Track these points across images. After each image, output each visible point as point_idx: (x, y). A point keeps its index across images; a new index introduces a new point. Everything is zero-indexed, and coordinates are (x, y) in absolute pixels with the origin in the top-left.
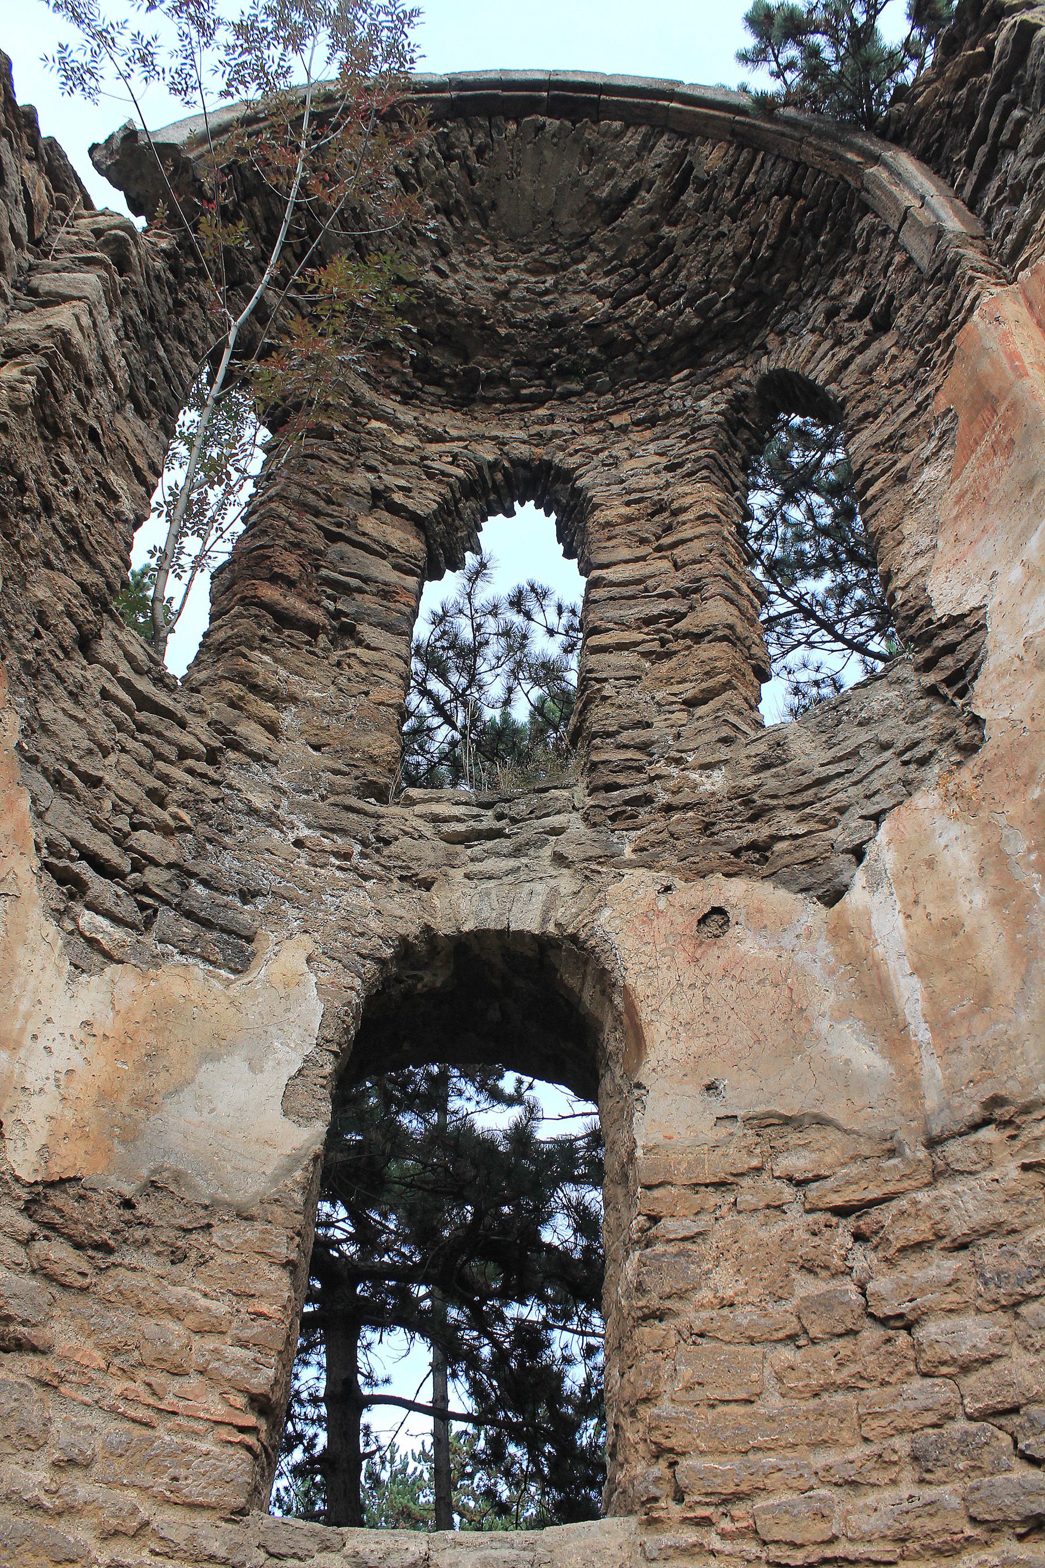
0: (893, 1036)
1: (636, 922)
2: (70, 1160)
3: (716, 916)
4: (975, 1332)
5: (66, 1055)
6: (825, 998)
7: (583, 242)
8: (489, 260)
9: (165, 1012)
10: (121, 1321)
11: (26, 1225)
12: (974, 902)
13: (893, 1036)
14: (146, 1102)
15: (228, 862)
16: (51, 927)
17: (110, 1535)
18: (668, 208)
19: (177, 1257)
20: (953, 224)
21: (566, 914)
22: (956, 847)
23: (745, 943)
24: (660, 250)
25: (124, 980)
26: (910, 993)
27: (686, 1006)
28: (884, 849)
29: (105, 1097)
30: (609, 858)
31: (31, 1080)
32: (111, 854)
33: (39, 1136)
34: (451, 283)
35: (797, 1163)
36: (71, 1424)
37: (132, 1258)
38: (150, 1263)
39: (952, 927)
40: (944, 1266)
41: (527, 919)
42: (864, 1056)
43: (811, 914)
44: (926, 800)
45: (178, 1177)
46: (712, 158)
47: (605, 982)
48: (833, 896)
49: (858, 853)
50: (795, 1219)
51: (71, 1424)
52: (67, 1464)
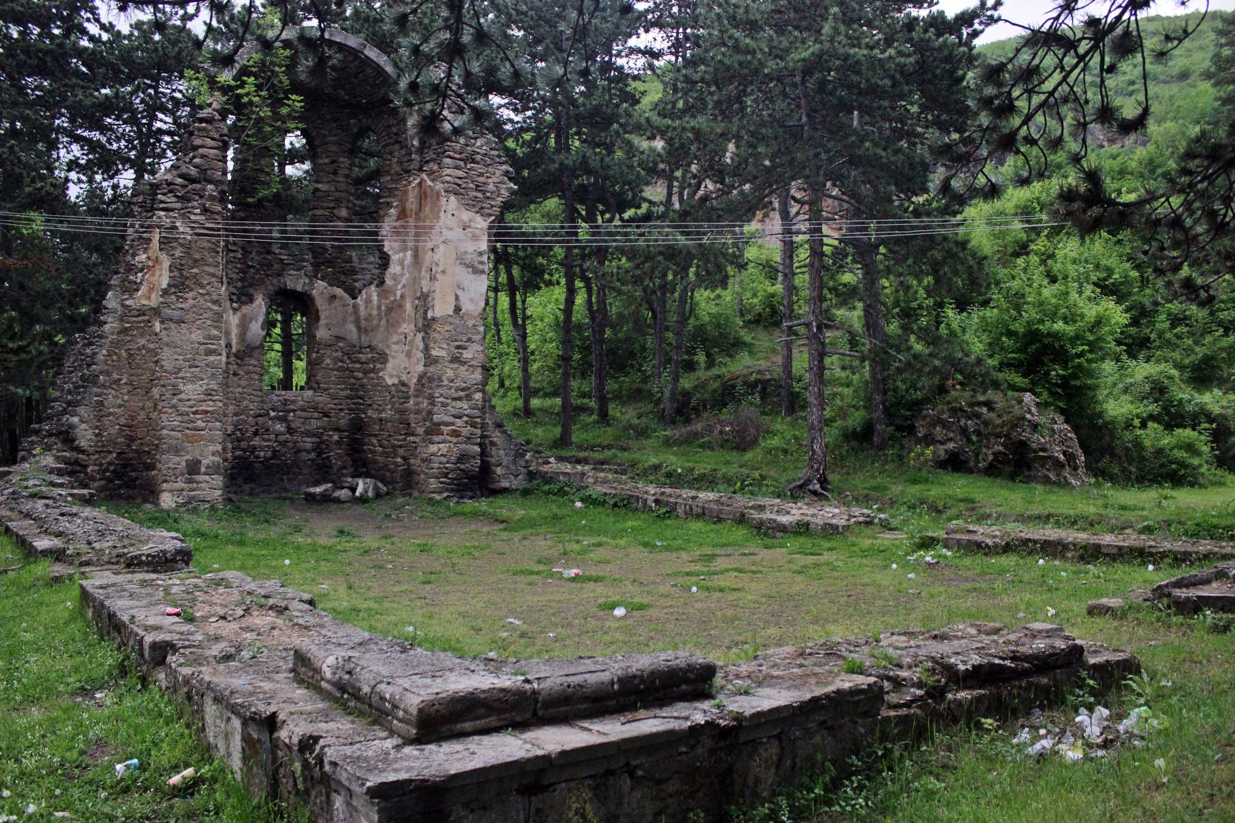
3: (334, 297)
4: (360, 375)
10: (246, 368)
12: (375, 312)
27: (327, 313)
35: (341, 344)
36: (243, 383)
39: (370, 315)
40: (358, 366)
41: (299, 288)
44: (373, 288)
48: (355, 298)
49: (360, 292)
50: (339, 354)
51: (243, 383)
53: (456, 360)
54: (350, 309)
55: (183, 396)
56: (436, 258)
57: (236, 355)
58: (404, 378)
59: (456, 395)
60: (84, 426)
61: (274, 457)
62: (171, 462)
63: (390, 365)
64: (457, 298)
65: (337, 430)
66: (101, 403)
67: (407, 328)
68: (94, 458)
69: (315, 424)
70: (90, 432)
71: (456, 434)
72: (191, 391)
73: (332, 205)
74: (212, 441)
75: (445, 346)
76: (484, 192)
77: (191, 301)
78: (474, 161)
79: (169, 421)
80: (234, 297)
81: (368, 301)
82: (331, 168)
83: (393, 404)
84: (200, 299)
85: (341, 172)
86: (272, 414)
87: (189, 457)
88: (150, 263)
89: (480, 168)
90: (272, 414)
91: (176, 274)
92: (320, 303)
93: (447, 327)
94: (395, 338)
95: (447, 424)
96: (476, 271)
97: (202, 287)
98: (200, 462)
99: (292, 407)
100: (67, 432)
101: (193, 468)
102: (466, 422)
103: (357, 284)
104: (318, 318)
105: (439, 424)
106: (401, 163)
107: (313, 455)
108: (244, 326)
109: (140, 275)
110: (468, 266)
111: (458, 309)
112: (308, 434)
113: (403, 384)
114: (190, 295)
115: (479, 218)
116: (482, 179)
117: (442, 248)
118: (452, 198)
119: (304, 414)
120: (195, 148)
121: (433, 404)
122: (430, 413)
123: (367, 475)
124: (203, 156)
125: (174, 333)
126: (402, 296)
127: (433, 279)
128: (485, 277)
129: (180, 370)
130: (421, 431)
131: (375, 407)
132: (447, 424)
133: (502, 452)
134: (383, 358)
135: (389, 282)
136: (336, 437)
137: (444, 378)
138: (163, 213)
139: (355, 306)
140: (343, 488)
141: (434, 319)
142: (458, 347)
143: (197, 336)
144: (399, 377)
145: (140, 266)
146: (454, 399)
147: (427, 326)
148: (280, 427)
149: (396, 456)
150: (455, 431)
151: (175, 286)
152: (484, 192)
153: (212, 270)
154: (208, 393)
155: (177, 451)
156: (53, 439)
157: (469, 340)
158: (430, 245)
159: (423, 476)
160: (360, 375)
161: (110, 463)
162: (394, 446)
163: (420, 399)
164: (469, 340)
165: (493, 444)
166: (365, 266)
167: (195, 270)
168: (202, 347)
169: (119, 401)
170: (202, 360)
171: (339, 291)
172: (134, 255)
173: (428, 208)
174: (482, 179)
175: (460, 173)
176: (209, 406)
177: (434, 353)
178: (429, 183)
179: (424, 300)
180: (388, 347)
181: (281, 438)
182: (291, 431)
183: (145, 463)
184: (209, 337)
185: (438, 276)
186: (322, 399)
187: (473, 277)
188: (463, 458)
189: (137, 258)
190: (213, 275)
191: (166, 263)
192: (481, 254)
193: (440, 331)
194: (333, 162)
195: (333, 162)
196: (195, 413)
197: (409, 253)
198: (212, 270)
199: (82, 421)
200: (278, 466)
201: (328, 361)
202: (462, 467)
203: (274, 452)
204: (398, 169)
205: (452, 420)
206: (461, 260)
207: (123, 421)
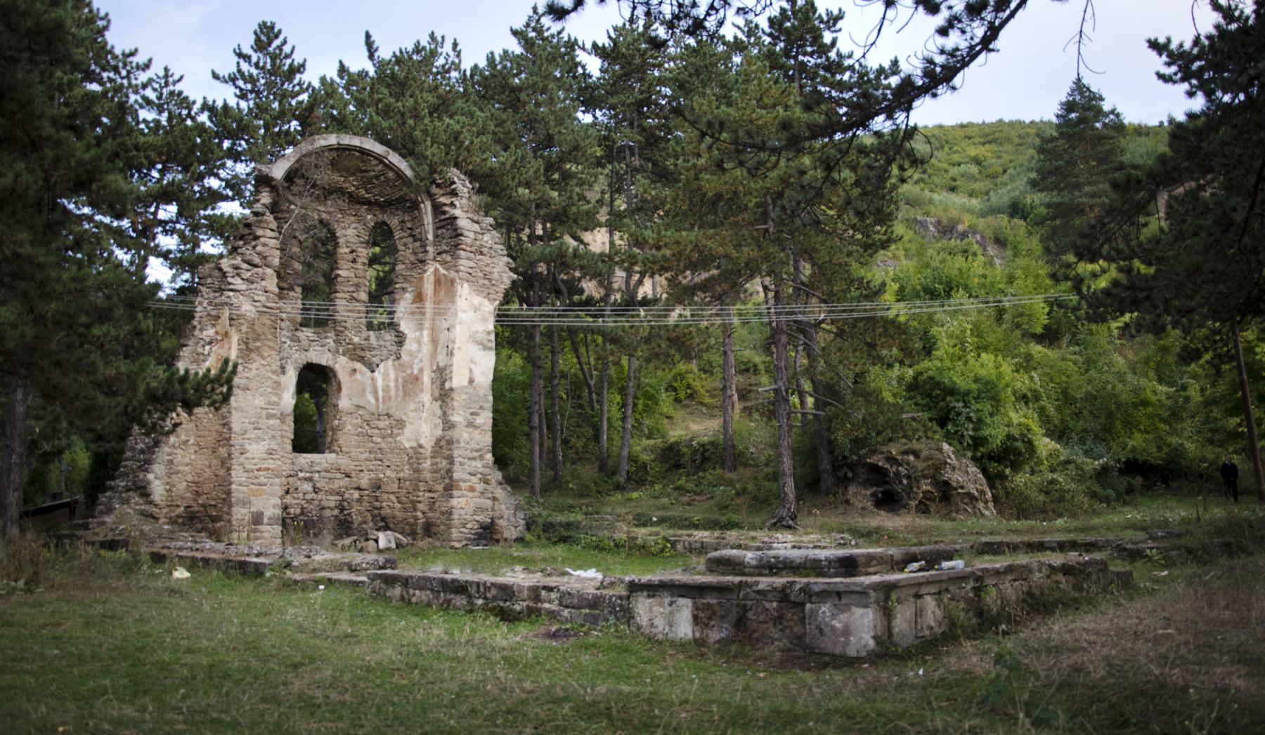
0: (377, 400)
1: (341, 365)
3: (355, 370)
4: (379, 440)
6: (369, 389)
7: (353, 174)
12: (392, 384)
13: (377, 400)
18: (377, 177)
20: (430, 237)
21: (330, 363)
22: (392, 375)
23: (358, 376)
24: (370, 182)
26: (381, 394)
28: (381, 366)
30: (338, 352)
41: (324, 363)
42: (373, 401)
43: (369, 374)
44: (390, 362)
46: (391, 174)
47: (335, 376)
50: (359, 421)
53: (471, 425)
54: (369, 381)
55: (248, 455)
56: (452, 336)
58: (423, 441)
60: (157, 482)
61: (302, 513)
62: (240, 514)
63: (408, 430)
64: (471, 371)
65: (358, 489)
66: (171, 462)
67: (426, 397)
68: (165, 511)
69: (336, 485)
70: (162, 487)
71: (472, 489)
72: (256, 450)
73: (352, 289)
74: (273, 495)
76: (490, 280)
77: (254, 372)
78: (481, 253)
79: (238, 475)
81: (386, 375)
82: (351, 257)
83: (411, 464)
84: (262, 369)
85: (360, 260)
86: (301, 475)
87: (254, 509)
88: (219, 338)
89: (486, 259)
90: (301, 475)
91: (243, 347)
92: (342, 375)
93: (464, 397)
94: (412, 406)
95: (464, 481)
96: (485, 348)
97: (263, 358)
98: (262, 514)
99: (317, 468)
100: (145, 488)
101: (257, 519)
103: (376, 360)
104: (339, 389)
105: (458, 481)
106: (415, 254)
107: (336, 512)
109: (207, 348)
110: (479, 344)
111: (471, 381)
112: (331, 492)
113: (421, 446)
114: (254, 366)
115: (487, 303)
116: (488, 269)
117: (458, 327)
118: (466, 285)
119: (328, 475)
120: (257, 238)
121: (452, 463)
122: (449, 471)
123: (386, 528)
124: (265, 245)
125: (240, 398)
126: (421, 370)
127: (450, 354)
129: (246, 432)
130: (440, 487)
131: (393, 467)
133: (503, 507)
134: (401, 424)
135: (405, 358)
136: (356, 495)
138: (231, 294)
139: (373, 379)
140: (367, 540)
141: (451, 389)
142: (472, 414)
143: (259, 401)
144: (417, 440)
145: (208, 340)
147: (444, 395)
148: (307, 487)
149: (415, 510)
151: (242, 358)
152: (490, 280)
153: (271, 344)
154: (270, 453)
155: (245, 503)
156: (131, 493)
157: (481, 407)
158: (445, 325)
159: (442, 527)
160: (379, 440)
161: (178, 516)
162: (414, 503)
163: (438, 460)
164: (481, 407)
166: (382, 343)
167: (258, 344)
168: (264, 412)
169: (187, 460)
170: (264, 423)
171: (358, 365)
172: (201, 330)
173: (442, 293)
174: (488, 269)
175: (472, 264)
176: (270, 464)
177: (452, 418)
178: (443, 271)
179: (442, 374)
180: (405, 414)
181: (309, 497)
182: (316, 490)
183: (210, 516)
184: (270, 403)
185: (455, 352)
186: (344, 462)
187: (483, 353)
188: (479, 509)
189: (205, 333)
190: (273, 348)
191: (235, 338)
192: (489, 333)
193: (458, 400)
194: (352, 252)
195: (352, 252)
196: (258, 470)
197: (426, 333)
198: (271, 344)
199: (156, 478)
200: (305, 522)
201: (349, 427)
202: (478, 518)
203: (302, 508)
204: (412, 258)
205: (469, 477)
206: (473, 338)
207: (190, 478)
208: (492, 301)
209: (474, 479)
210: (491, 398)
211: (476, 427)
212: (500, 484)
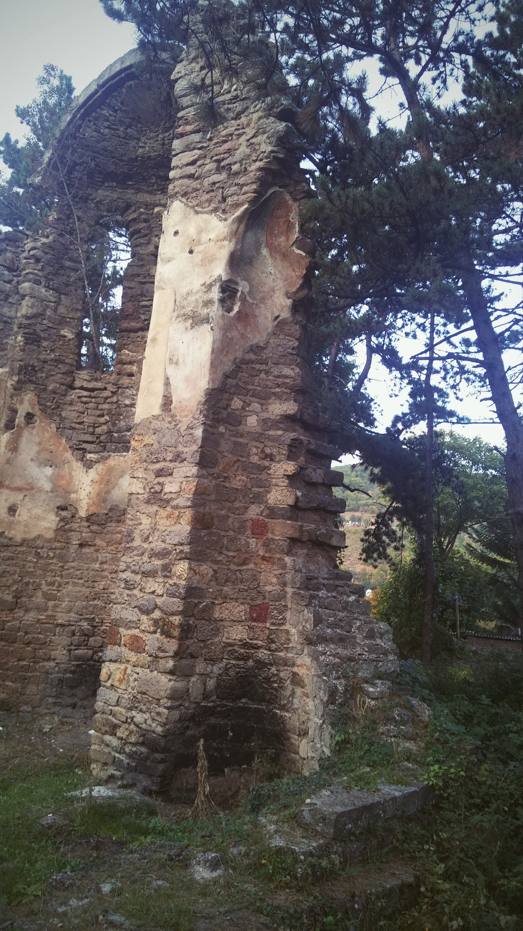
2: (93, 510)
5: (88, 489)
8: (152, 135)
9: (110, 470)
11: (86, 524)
14: (108, 492)
15: (122, 423)
16: (79, 464)
17: (111, 573)
19: (119, 521)
25: (99, 467)
29: (98, 494)
31: (82, 497)
32: (89, 438)
33: (85, 508)
34: (147, 148)
36: (101, 557)
37: (109, 524)
38: (113, 524)
45: (117, 506)
51: (101, 557)
52: (101, 563)
53: (156, 498)
57: (88, 519)
59: (147, 567)
71: (136, 645)
75: (140, 474)
80: (85, 446)
95: (128, 625)
102: (156, 622)
105: (116, 624)
108: (107, 483)
111: (167, 402)
128: (206, 327)
132: (128, 625)
137: (136, 534)
142: (159, 473)
146: (146, 574)
150: (136, 638)
165: (297, 681)
187: (191, 334)
202: (139, 718)
208: (221, 209)
209: (146, 621)
210: (199, 432)
211: (164, 503)
212: (310, 642)
